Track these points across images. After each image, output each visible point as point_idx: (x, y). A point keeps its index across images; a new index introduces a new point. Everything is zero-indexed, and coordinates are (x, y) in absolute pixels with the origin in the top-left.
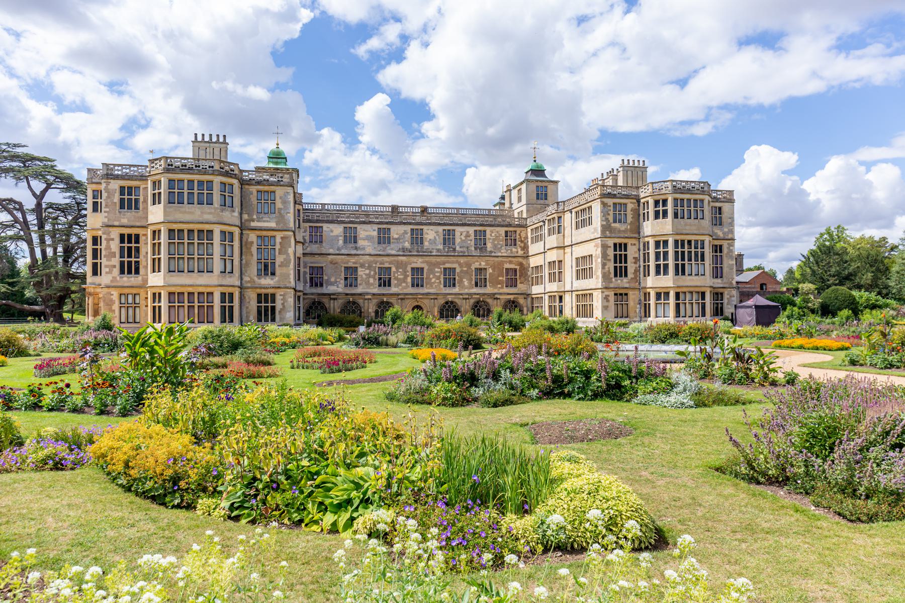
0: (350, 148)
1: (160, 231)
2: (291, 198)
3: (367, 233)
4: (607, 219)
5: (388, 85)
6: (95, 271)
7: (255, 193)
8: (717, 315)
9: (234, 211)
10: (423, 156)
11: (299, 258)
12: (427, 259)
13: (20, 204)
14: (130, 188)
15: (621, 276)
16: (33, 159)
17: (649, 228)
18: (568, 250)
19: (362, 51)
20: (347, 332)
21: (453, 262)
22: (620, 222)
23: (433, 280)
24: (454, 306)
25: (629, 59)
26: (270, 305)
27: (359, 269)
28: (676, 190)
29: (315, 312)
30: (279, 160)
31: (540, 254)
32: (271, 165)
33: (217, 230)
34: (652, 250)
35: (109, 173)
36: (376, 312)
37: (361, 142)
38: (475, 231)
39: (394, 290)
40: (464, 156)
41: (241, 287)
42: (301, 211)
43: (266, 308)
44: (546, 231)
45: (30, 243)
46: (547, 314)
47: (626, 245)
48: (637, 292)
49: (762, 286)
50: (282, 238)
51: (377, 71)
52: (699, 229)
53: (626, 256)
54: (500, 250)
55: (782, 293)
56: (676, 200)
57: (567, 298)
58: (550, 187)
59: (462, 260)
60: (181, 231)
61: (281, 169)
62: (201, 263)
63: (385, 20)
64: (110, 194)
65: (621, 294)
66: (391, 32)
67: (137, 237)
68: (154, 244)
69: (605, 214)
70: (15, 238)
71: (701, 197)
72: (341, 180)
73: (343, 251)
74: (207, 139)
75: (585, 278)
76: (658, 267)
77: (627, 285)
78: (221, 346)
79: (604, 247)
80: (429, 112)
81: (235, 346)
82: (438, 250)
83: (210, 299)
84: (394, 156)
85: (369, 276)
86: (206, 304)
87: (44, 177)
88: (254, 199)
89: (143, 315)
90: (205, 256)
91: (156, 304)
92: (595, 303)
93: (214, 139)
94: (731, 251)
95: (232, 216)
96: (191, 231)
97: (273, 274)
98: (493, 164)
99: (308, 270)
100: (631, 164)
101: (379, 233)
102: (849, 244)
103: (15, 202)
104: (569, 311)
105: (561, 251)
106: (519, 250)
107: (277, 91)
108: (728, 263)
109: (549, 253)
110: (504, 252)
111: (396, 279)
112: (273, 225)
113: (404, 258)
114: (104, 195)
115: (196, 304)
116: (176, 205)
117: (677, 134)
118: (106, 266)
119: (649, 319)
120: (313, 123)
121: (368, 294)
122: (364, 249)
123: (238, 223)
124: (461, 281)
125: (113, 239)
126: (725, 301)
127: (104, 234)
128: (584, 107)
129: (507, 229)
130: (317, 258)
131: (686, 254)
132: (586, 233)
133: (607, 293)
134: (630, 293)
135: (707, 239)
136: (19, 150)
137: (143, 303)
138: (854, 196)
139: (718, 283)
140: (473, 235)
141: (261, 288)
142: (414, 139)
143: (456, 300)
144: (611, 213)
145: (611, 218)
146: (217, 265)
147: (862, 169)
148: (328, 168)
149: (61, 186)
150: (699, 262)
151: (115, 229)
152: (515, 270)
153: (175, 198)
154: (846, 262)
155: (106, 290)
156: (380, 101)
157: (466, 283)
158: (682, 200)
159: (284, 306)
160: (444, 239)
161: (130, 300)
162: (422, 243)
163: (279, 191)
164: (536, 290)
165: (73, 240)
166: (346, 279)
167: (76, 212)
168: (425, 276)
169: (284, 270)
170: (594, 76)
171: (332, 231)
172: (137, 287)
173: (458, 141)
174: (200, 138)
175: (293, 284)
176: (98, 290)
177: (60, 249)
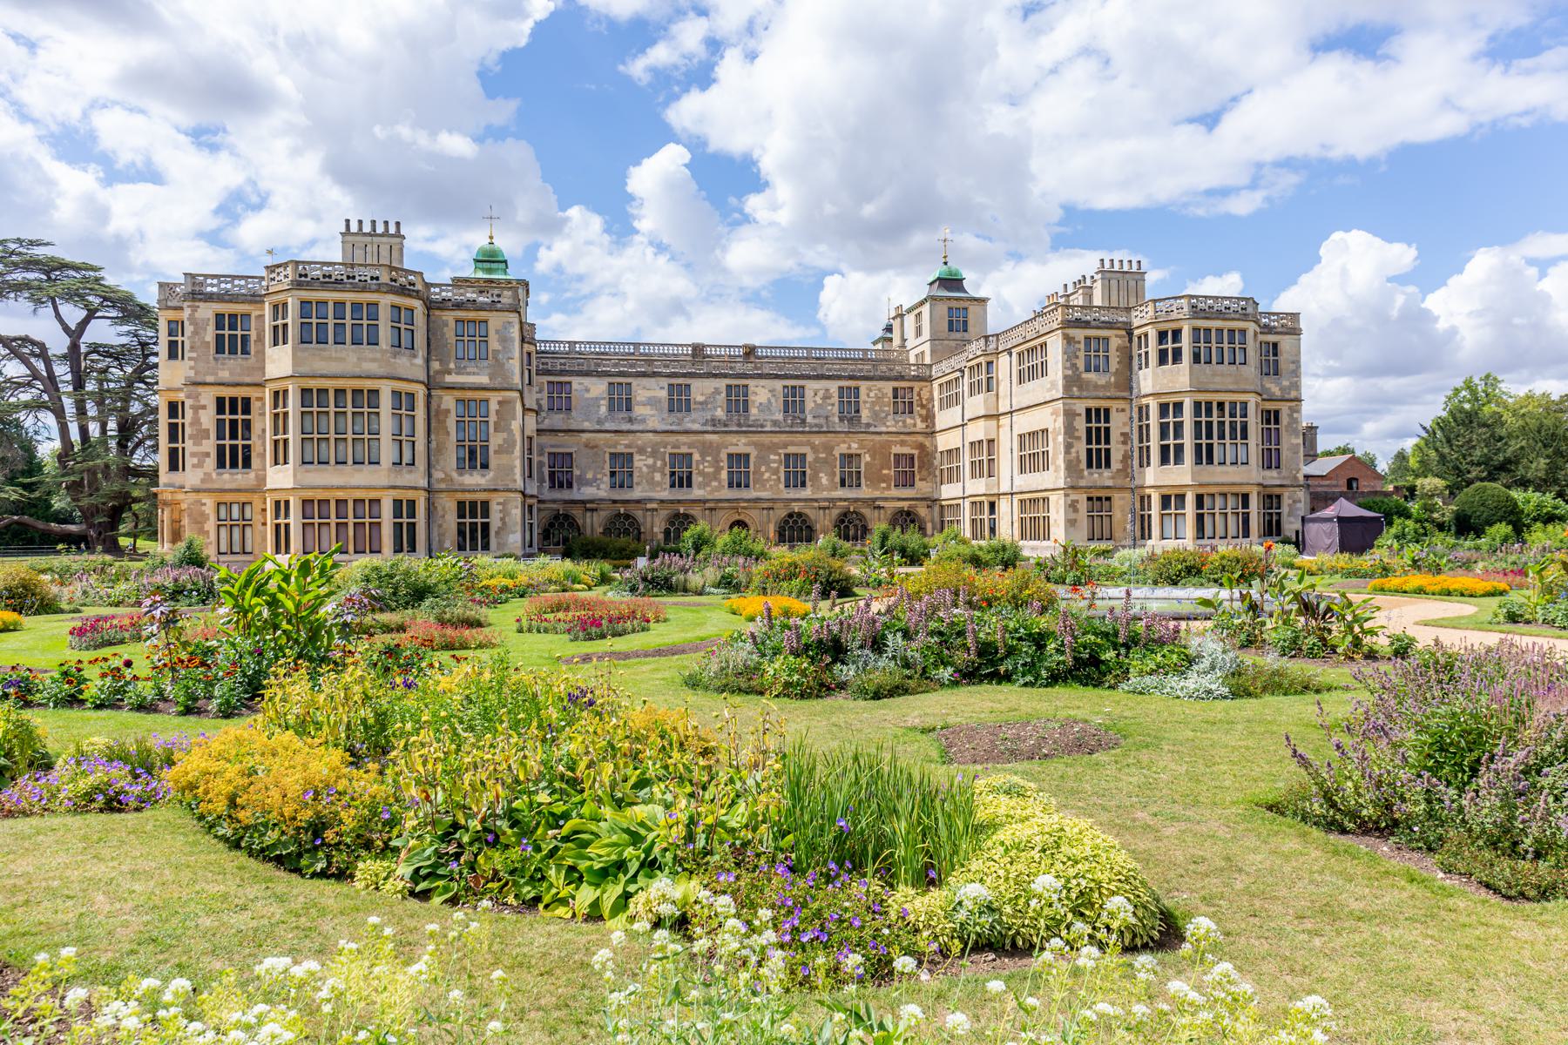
0: (617, 243)
1: (286, 392)
2: (515, 333)
3: (649, 393)
4: (1074, 366)
5: (684, 129)
7: (452, 324)
8: (1270, 534)
9: (415, 356)
10: (747, 254)
11: (530, 438)
12: (756, 438)
13: (42, 346)
14: (233, 317)
15: (1099, 466)
16: (64, 266)
17: (1150, 380)
18: (1005, 421)
19: (638, 68)
20: (616, 567)
21: (801, 444)
22: (1097, 369)
23: (767, 475)
24: (804, 521)
25: (1114, 77)
26: (479, 520)
27: (636, 457)
28: (1196, 312)
29: (558, 533)
30: (494, 266)
31: (955, 426)
32: (480, 275)
33: (386, 389)
34: (1154, 421)
35: (196, 290)
36: (667, 533)
37: (637, 232)
38: (841, 388)
39: (697, 493)
40: (819, 255)
41: (429, 490)
42: (534, 356)
43: (473, 526)
44: (966, 388)
45: (59, 413)
46: (968, 534)
47: (1107, 411)
48: (1128, 495)
49: (1350, 482)
50: (500, 403)
51: (666, 104)
52: (1239, 382)
53: (1107, 430)
54: (883, 421)
55: (1387, 494)
56: (1196, 330)
57: (1003, 506)
58: (973, 309)
59: (817, 440)
60: (323, 392)
61: (498, 282)
62: (359, 447)
63: (680, 13)
64: (199, 328)
65: (1099, 499)
66: (691, 35)
67: (247, 402)
68: (276, 415)
69: (1070, 357)
70: (35, 406)
71: (1241, 325)
72: (603, 300)
73: (608, 426)
74: (367, 228)
75: (1035, 470)
76: (1164, 450)
77: (1110, 483)
78: (394, 594)
79: (1069, 415)
80: (757, 175)
81: (419, 594)
82: (775, 423)
83: (375, 512)
84: (695, 255)
85: (653, 468)
86: (367, 520)
87: (82, 297)
88: (450, 334)
89: (258, 539)
90: (366, 436)
91: (281, 521)
92: (1053, 515)
93: (380, 229)
94: (1296, 421)
95: (413, 365)
96: (340, 392)
97: (485, 466)
98: (872, 268)
99: (545, 459)
100: (1117, 268)
101: (670, 394)
102: (1506, 407)
103: (34, 343)
104: (1007, 529)
105: (994, 423)
106: (918, 421)
107: (490, 141)
108: (1290, 443)
109: (970, 427)
110: (891, 425)
111: (701, 473)
112: (484, 380)
113: (714, 437)
114: (189, 329)
115: (351, 520)
116: (314, 345)
117: (1201, 212)
118: (193, 455)
119: (1150, 542)
120: (554, 198)
121: (651, 500)
122: (643, 421)
123: (423, 377)
124: (815, 477)
125: (204, 407)
126: (1285, 510)
127: (188, 397)
128: (1035, 165)
129: (896, 384)
130: (562, 438)
131: (1215, 427)
132: (1037, 390)
133: (1074, 497)
134: (1116, 496)
135: (1252, 400)
136: (39, 252)
137: (257, 518)
138: (1517, 321)
139: (1272, 477)
140: (836, 395)
141: (464, 491)
142: (730, 225)
143: (808, 511)
144: (1082, 354)
145: (1081, 364)
146: (387, 452)
147: (1533, 272)
148: (580, 278)
149: (114, 313)
150: (1239, 441)
151: (207, 388)
152: (912, 457)
153: (312, 335)
154: (1501, 439)
155: (193, 496)
156: (670, 159)
157: (824, 480)
158: (1208, 330)
159: (504, 523)
160: (786, 403)
161: (235, 515)
162: (746, 410)
163: (495, 320)
164: (948, 491)
165: (135, 408)
166: (613, 474)
167: (140, 359)
168: (752, 469)
169: (504, 459)
170: (1053, 110)
171: (588, 390)
172: (246, 491)
173: (811, 228)
174: (354, 228)
175: (519, 484)
176: (180, 497)
177: (112, 425)
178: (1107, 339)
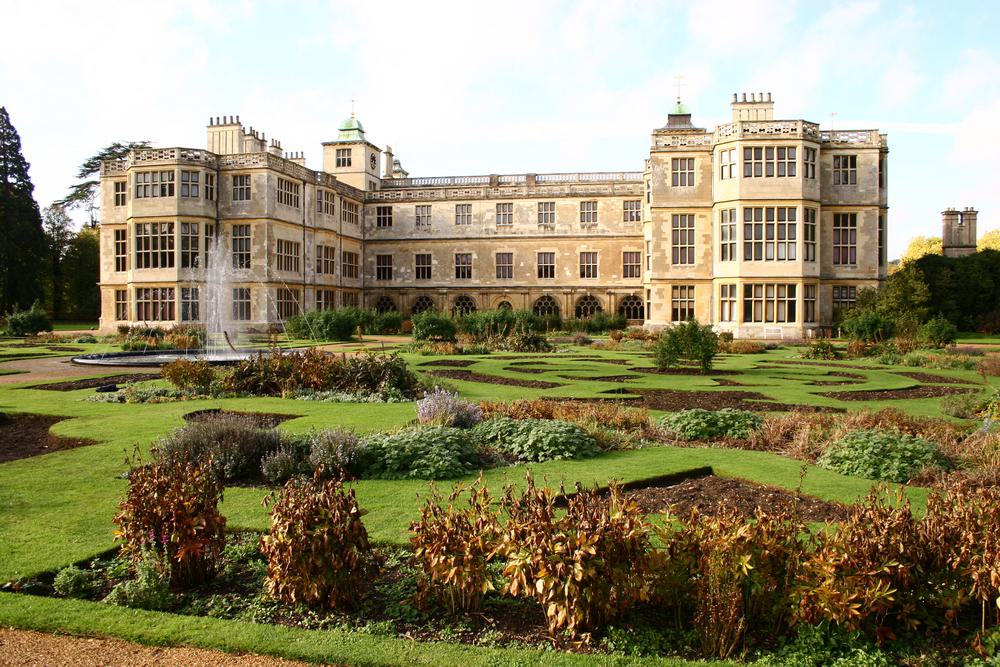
48: (707, 285)
50: (256, 226)
65: (683, 288)
100: (749, 99)
145: (669, 182)
158: (758, 149)
178: (692, 159)
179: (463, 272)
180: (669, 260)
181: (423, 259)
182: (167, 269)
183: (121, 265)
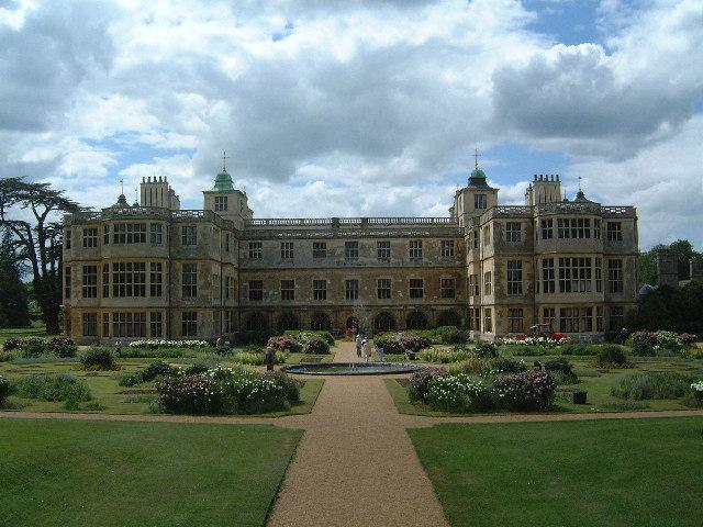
6: (68, 296)
39: (329, 302)
52: (590, 247)
71: (586, 217)
77: (521, 301)
79: (497, 265)
144: (505, 233)
145: (504, 238)
158: (567, 221)
175: (216, 302)
179: (320, 294)
180: (506, 292)
181: (289, 284)
182: (140, 298)
183: (89, 293)
